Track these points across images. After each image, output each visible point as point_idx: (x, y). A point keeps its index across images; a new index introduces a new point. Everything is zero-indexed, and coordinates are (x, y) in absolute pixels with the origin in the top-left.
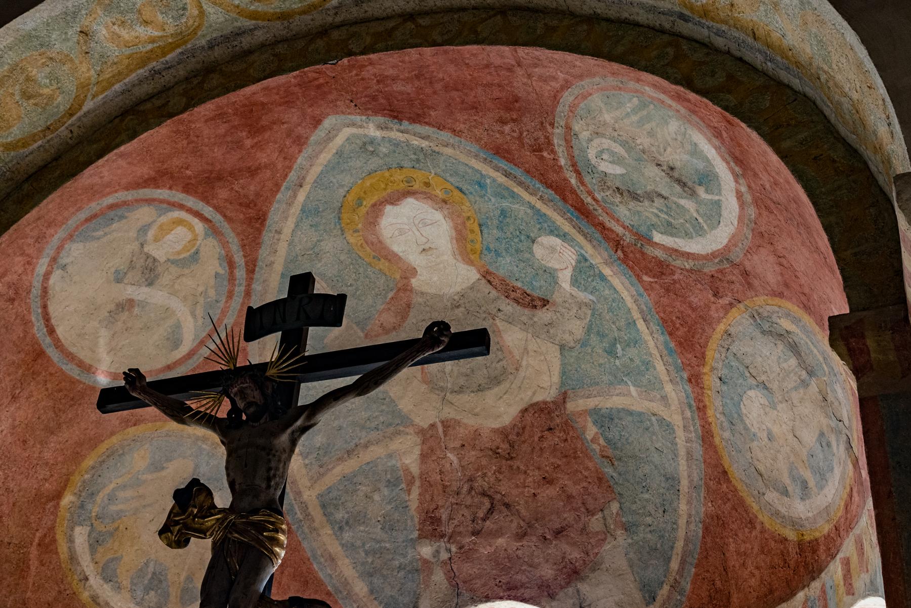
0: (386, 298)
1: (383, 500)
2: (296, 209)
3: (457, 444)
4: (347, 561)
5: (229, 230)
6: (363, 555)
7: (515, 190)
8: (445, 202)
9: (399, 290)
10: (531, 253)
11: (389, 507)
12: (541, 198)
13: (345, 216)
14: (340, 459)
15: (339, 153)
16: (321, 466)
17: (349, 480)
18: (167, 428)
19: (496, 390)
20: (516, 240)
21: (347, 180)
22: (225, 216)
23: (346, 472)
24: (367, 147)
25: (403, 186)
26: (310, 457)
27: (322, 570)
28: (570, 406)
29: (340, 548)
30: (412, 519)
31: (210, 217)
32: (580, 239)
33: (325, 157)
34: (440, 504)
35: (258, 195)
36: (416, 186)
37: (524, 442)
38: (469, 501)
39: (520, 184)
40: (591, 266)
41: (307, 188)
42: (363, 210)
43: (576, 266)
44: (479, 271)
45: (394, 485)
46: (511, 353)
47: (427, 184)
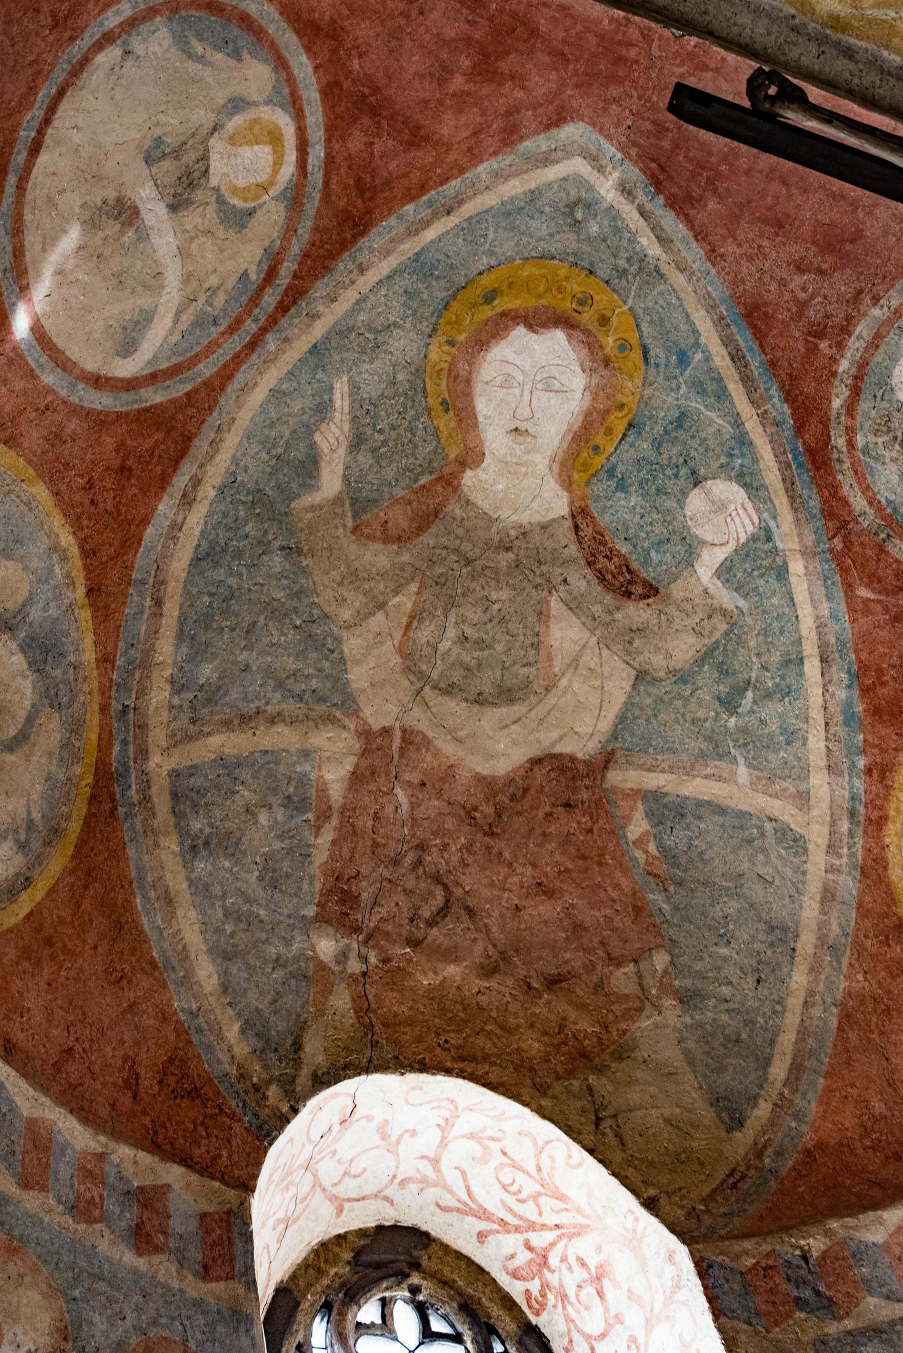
0: (416, 481)
1: (271, 828)
2: (409, 248)
3: (416, 778)
4: (193, 914)
5: (312, 212)
6: (220, 913)
7: (731, 387)
8: (607, 362)
9: (438, 479)
10: (681, 503)
11: (277, 845)
12: (763, 416)
13: (455, 306)
14: (227, 724)
15: (534, 195)
16: (193, 721)
17: (229, 767)
18: (33, 490)
19: (503, 711)
20: (669, 472)
21: (508, 247)
22: (326, 183)
23: (227, 751)
24: (577, 206)
25: (568, 305)
26: (184, 695)
27: (148, 913)
28: (616, 777)
29: (185, 885)
30: (311, 883)
31: (309, 168)
32: (782, 502)
33: (515, 188)
34: (364, 871)
35: (388, 183)
36: (588, 317)
37: (520, 813)
38: (410, 884)
39: (747, 380)
40: (775, 551)
41: (453, 221)
42: (487, 312)
43: (745, 545)
44: (571, 503)
45: (297, 809)
46: (550, 658)
47: (604, 321)
